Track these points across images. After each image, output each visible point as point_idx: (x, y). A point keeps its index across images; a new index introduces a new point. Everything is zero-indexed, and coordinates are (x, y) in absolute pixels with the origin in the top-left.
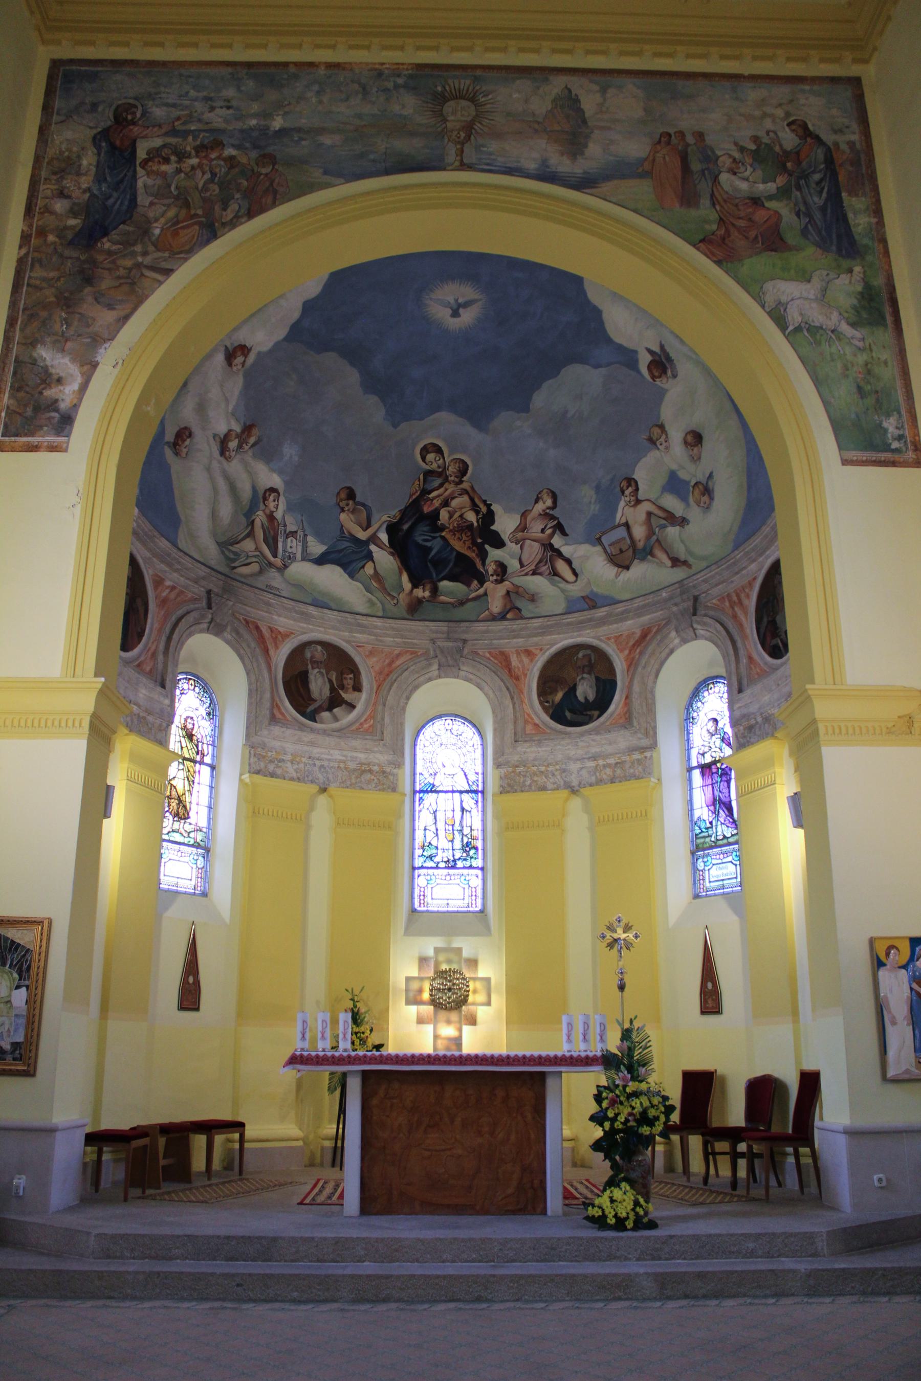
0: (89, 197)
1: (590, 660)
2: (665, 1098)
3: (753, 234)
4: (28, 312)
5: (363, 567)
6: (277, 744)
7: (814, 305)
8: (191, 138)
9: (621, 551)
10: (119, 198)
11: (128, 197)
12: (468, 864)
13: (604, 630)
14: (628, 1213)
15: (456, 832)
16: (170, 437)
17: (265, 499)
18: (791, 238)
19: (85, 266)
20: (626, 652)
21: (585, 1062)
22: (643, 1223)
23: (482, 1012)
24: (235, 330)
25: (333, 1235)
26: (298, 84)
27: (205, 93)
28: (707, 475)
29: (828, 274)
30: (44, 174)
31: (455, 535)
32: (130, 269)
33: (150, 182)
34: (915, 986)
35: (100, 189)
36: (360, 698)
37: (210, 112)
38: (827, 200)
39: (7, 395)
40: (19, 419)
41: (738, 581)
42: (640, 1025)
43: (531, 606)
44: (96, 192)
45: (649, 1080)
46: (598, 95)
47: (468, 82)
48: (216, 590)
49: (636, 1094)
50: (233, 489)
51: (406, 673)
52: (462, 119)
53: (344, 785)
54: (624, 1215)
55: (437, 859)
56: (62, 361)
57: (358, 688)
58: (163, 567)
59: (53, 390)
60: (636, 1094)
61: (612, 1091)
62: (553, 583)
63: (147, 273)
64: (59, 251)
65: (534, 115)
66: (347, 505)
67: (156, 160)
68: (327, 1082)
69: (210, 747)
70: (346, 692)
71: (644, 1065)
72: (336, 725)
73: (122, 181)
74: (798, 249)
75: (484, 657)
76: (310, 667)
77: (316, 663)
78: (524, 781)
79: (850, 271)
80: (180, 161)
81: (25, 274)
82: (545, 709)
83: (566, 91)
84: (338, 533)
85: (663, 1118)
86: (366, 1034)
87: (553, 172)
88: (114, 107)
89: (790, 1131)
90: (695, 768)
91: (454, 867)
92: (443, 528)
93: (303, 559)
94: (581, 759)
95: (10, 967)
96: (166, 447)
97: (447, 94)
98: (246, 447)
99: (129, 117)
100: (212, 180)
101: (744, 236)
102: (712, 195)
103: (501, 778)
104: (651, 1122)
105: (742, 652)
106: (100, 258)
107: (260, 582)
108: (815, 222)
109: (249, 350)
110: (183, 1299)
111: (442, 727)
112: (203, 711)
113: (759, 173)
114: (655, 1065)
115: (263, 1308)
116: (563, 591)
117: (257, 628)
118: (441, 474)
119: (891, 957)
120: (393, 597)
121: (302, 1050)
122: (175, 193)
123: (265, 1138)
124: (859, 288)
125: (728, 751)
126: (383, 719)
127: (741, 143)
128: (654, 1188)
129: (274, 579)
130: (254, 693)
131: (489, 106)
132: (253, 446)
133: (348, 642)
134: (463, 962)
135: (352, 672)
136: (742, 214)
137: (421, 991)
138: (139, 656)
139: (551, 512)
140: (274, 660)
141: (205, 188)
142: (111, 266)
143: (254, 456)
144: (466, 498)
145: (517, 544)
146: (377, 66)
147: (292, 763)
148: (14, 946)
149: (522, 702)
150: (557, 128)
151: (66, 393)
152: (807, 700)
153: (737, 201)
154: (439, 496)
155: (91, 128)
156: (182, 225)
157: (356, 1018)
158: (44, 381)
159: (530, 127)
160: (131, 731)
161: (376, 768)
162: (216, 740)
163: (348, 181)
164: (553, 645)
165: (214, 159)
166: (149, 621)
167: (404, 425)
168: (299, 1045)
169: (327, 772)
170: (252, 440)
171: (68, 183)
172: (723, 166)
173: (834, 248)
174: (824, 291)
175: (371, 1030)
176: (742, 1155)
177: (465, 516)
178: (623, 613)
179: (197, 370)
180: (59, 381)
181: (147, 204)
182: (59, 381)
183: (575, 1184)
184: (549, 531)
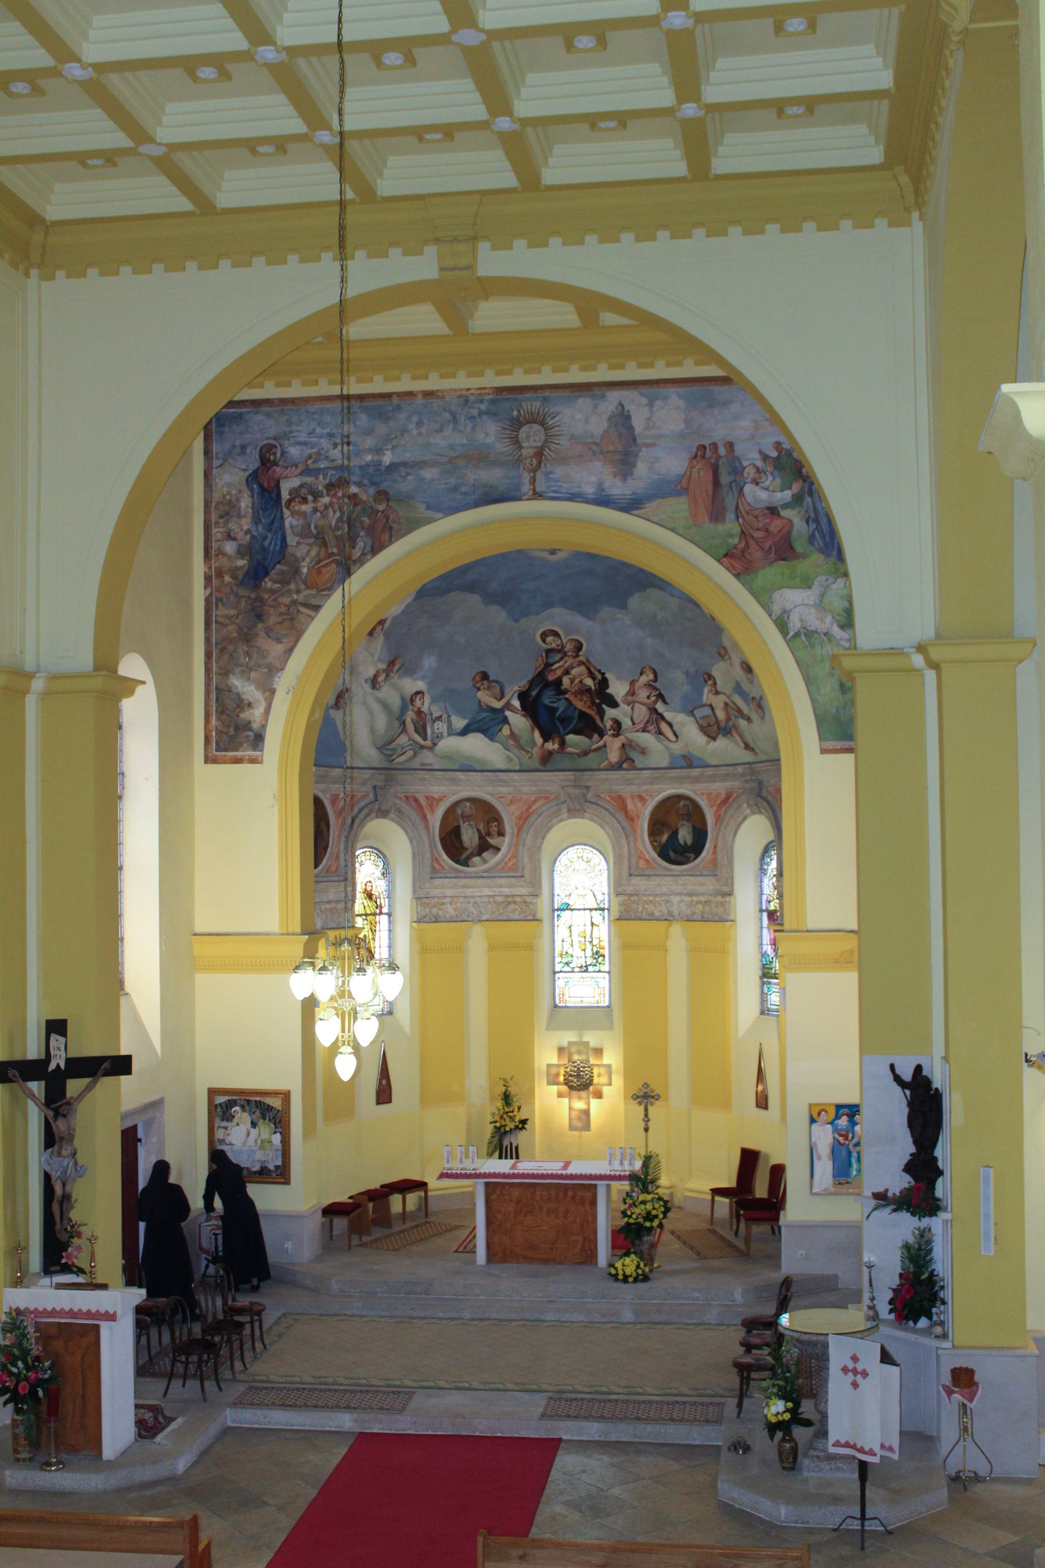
1: (688, 811)
3: (767, 545)
4: (219, 646)
5: (501, 730)
6: (438, 892)
7: (813, 610)
8: (321, 476)
9: (709, 725)
10: (272, 539)
11: (280, 537)
12: (597, 968)
13: (698, 786)
17: (412, 701)
18: (800, 546)
19: (256, 604)
20: (715, 808)
21: (620, 1178)
23: (606, 1090)
26: (401, 416)
27: (328, 430)
29: (827, 580)
30: (214, 517)
31: (576, 696)
32: (288, 606)
33: (295, 522)
34: (836, 1136)
35: (257, 530)
36: (504, 841)
37: (334, 448)
40: (225, 738)
43: (642, 758)
44: (255, 534)
46: (647, 409)
47: (538, 404)
48: (379, 784)
50: (385, 706)
51: (541, 818)
52: (535, 444)
55: (571, 965)
56: (250, 688)
57: (501, 834)
59: (246, 713)
62: (659, 741)
63: (302, 609)
64: (235, 590)
65: (593, 436)
66: (483, 684)
67: (297, 500)
69: (386, 900)
70: (492, 838)
72: (486, 867)
73: (272, 522)
74: (804, 556)
75: (606, 800)
76: (461, 822)
77: (466, 818)
78: (637, 908)
80: (315, 501)
81: (212, 611)
82: (654, 848)
83: (620, 408)
84: (477, 706)
86: (515, 1113)
87: (606, 495)
88: (259, 448)
90: (764, 911)
91: (586, 971)
92: (566, 692)
93: (449, 735)
94: (680, 894)
97: (521, 419)
100: (340, 519)
101: (762, 548)
102: (737, 508)
106: (266, 596)
107: (415, 763)
108: (821, 528)
111: (575, 856)
113: (778, 481)
116: (667, 748)
117: (416, 800)
118: (561, 651)
119: (821, 1116)
120: (527, 752)
122: (315, 532)
126: (523, 858)
129: (427, 757)
131: (556, 429)
132: (398, 670)
133: (492, 795)
134: (591, 1053)
135: (496, 820)
136: (761, 525)
137: (558, 1075)
139: (653, 684)
140: (431, 822)
141: (337, 528)
142: (275, 603)
143: (400, 677)
144: (583, 668)
145: (628, 705)
146: (464, 392)
148: (270, 1108)
149: (636, 840)
150: (611, 448)
151: (256, 714)
153: (757, 512)
154: (559, 667)
155: (244, 470)
156: (323, 563)
157: (507, 1098)
158: (239, 706)
159: (590, 449)
161: (518, 899)
162: (390, 895)
163: (448, 515)
164: (660, 793)
166: (331, 833)
168: (447, 1166)
170: (397, 667)
171: (232, 525)
172: (748, 477)
174: (822, 596)
175: (519, 1108)
177: (584, 681)
178: (712, 776)
180: (250, 705)
181: (295, 544)
182: (250, 705)
184: (653, 699)
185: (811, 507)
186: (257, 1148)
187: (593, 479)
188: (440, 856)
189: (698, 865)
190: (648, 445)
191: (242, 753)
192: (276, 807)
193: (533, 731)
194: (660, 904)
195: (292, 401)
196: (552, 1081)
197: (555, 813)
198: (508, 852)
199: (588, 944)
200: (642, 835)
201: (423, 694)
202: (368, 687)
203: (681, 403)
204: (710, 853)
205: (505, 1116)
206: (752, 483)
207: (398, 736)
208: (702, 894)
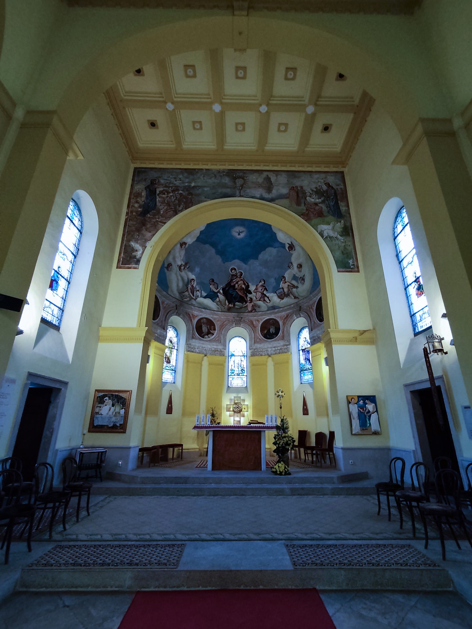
0: (144, 204)
2: (293, 438)
3: (315, 213)
5: (216, 299)
6: (194, 344)
7: (331, 231)
9: (281, 295)
13: (277, 315)
14: (283, 470)
15: (240, 367)
16: (166, 265)
17: (191, 282)
20: (283, 320)
22: (287, 473)
23: (246, 414)
24: (183, 238)
25: (204, 476)
28: (303, 275)
30: (132, 197)
32: (154, 222)
33: (160, 199)
38: (334, 203)
39: (122, 254)
41: (311, 302)
42: (286, 418)
43: (258, 309)
44: (146, 202)
45: (288, 433)
46: (275, 177)
47: (242, 174)
48: (178, 304)
49: (285, 437)
50: (183, 279)
51: (227, 326)
53: (211, 354)
54: (282, 471)
55: (234, 373)
57: (215, 330)
58: (164, 299)
59: (135, 253)
60: (285, 437)
61: (279, 436)
62: (264, 303)
63: (159, 223)
65: (259, 182)
68: (205, 433)
69: (177, 345)
71: (287, 429)
72: (209, 339)
77: (204, 323)
79: (341, 222)
82: (262, 335)
85: (292, 444)
89: (327, 448)
91: (239, 375)
92: (236, 289)
93: (201, 297)
95: (120, 403)
96: (165, 268)
98: (186, 268)
99: (155, 182)
100: (176, 199)
102: (305, 203)
103: (251, 353)
104: (289, 445)
105: (312, 321)
106: (147, 219)
107: (190, 303)
109: (186, 244)
110: (162, 495)
112: (175, 335)
113: (317, 197)
114: (290, 429)
115: (184, 497)
116: (266, 305)
117: (189, 314)
118: (236, 275)
119: (352, 401)
120: (224, 307)
121: (197, 424)
122: (166, 202)
123: (188, 448)
124: (343, 226)
125: (309, 346)
126: (221, 337)
127: (312, 189)
128: (290, 463)
129: (193, 302)
130: (188, 331)
132: (187, 268)
135: (213, 326)
137: (230, 408)
138: (158, 321)
144: (242, 281)
146: (219, 170)
147: (198, 349)
149: (256, 333)
150: (265, 186)
151: (138, 254)
152: (328, 333)
154: (235, 281)
155: (144, 185)
157: (213, 415)
158: (132, 251)
160: (155, 341)
161: (219, 350)
162: (178, 343)
163: (211, 200)
165: (177, 194)
167: (226, 263)
169: (207, 351)
170: (187, 267)
171: (138, 199)
173: (336, 216)
174: (333, 227)
175: (217, 419)
176: (314, 454)
178: (282, 311)
179: (173, 248)
180: (136, 251)
182: (136, 251)
183: (270, 461)
184: (263, 290)
185: (328, 203)
186: (113, 416)
187: (259, 193)
188: (195, 332)
189: (277, 338)
190: (277, 186)
191: (131, 266)
192: (142, 284)
193: (226, 301)
194: (264, 352)
195: (164, 169)
196: (228, 410)
197: (231, 325)
198: (216, 335)
199: (240, 367)
200: (258, 332)
201: (194, 281)
202: (178, 270)
203: (286, 176)
204: (282, 334)
205: (212, 420)
206: (309, 197)
207: (185, 292)
208: (279, 347)
